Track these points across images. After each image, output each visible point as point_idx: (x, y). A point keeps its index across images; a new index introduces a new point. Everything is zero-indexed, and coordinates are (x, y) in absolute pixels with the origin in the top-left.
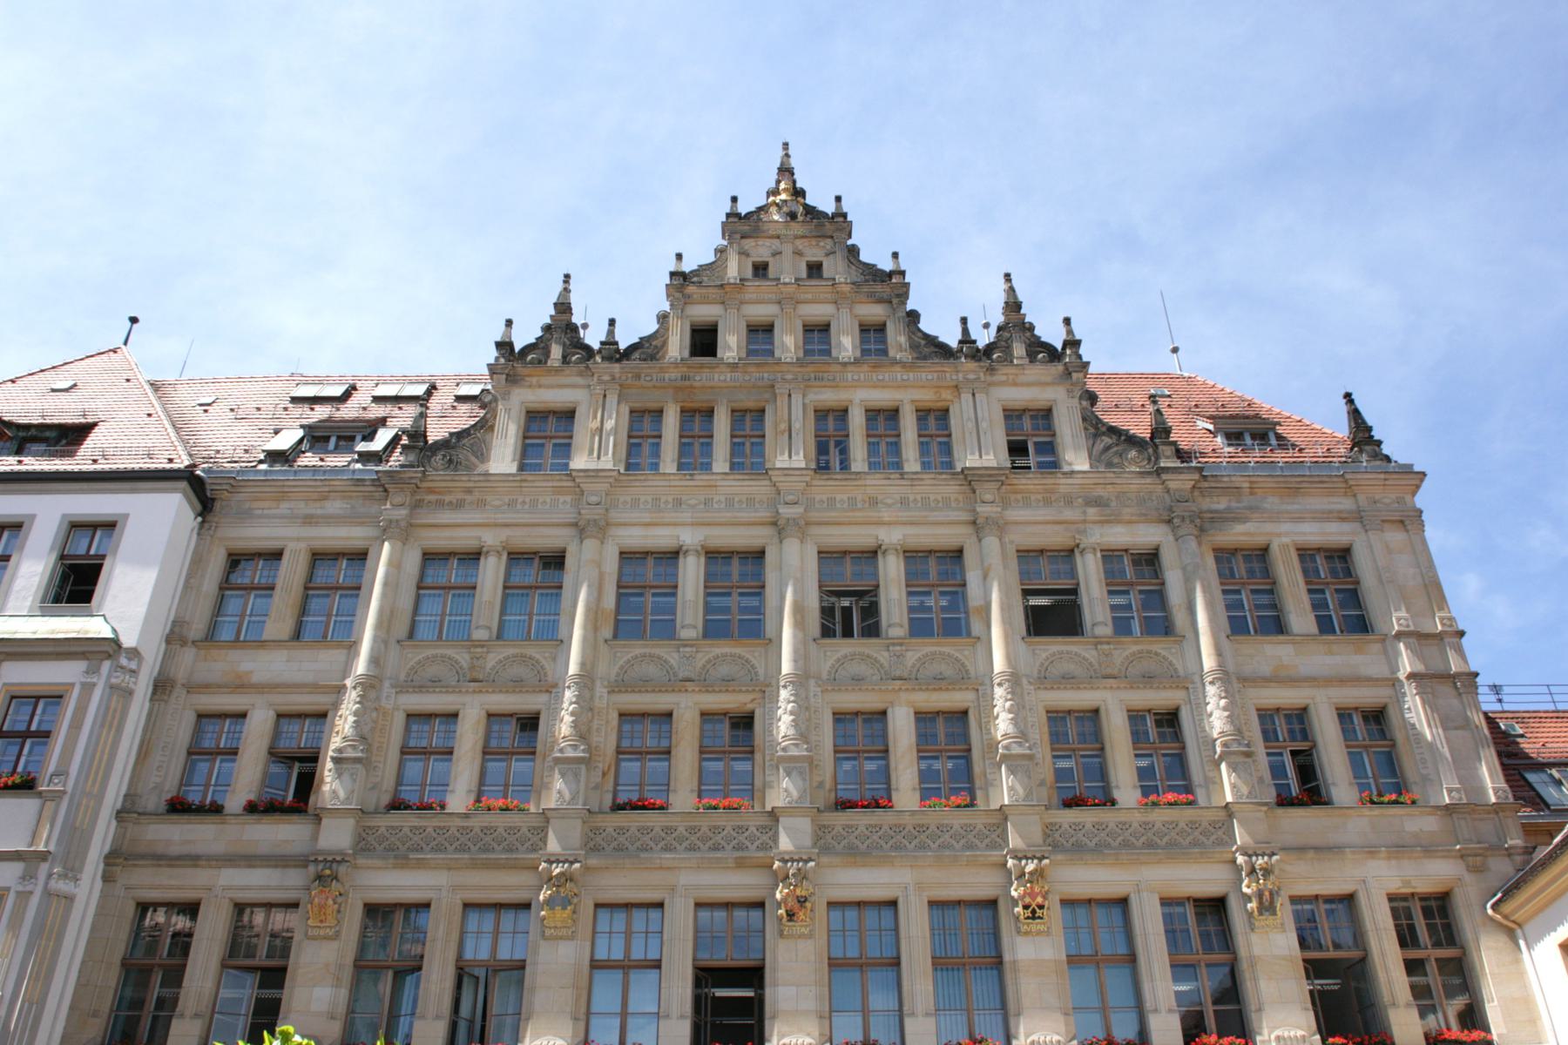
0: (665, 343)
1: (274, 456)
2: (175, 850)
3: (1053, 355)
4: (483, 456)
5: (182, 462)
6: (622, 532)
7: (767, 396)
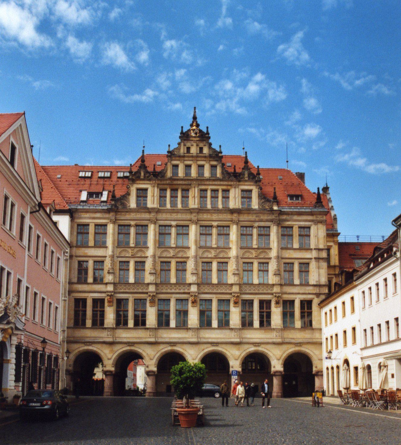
0: (166, 171)
2: (80, 290)
4: (129, 202)
6: (160, 222)
7: (189, 187)
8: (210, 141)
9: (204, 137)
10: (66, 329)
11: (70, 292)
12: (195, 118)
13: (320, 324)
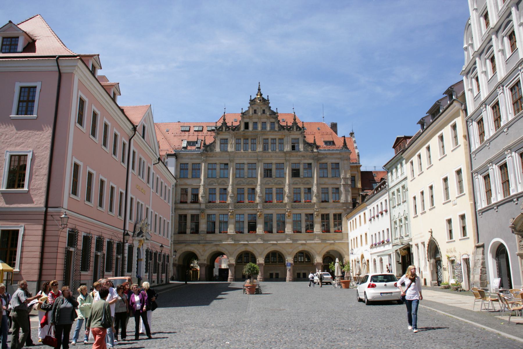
1: (184, 148)
3: (300, 129)
4: (215, 147)
5: (173, 152)
8: (270, 105)
9: (265, 102)
10: (173, 235)
11: (176, 209)
12: (259, 90)
13: (347, 230)
